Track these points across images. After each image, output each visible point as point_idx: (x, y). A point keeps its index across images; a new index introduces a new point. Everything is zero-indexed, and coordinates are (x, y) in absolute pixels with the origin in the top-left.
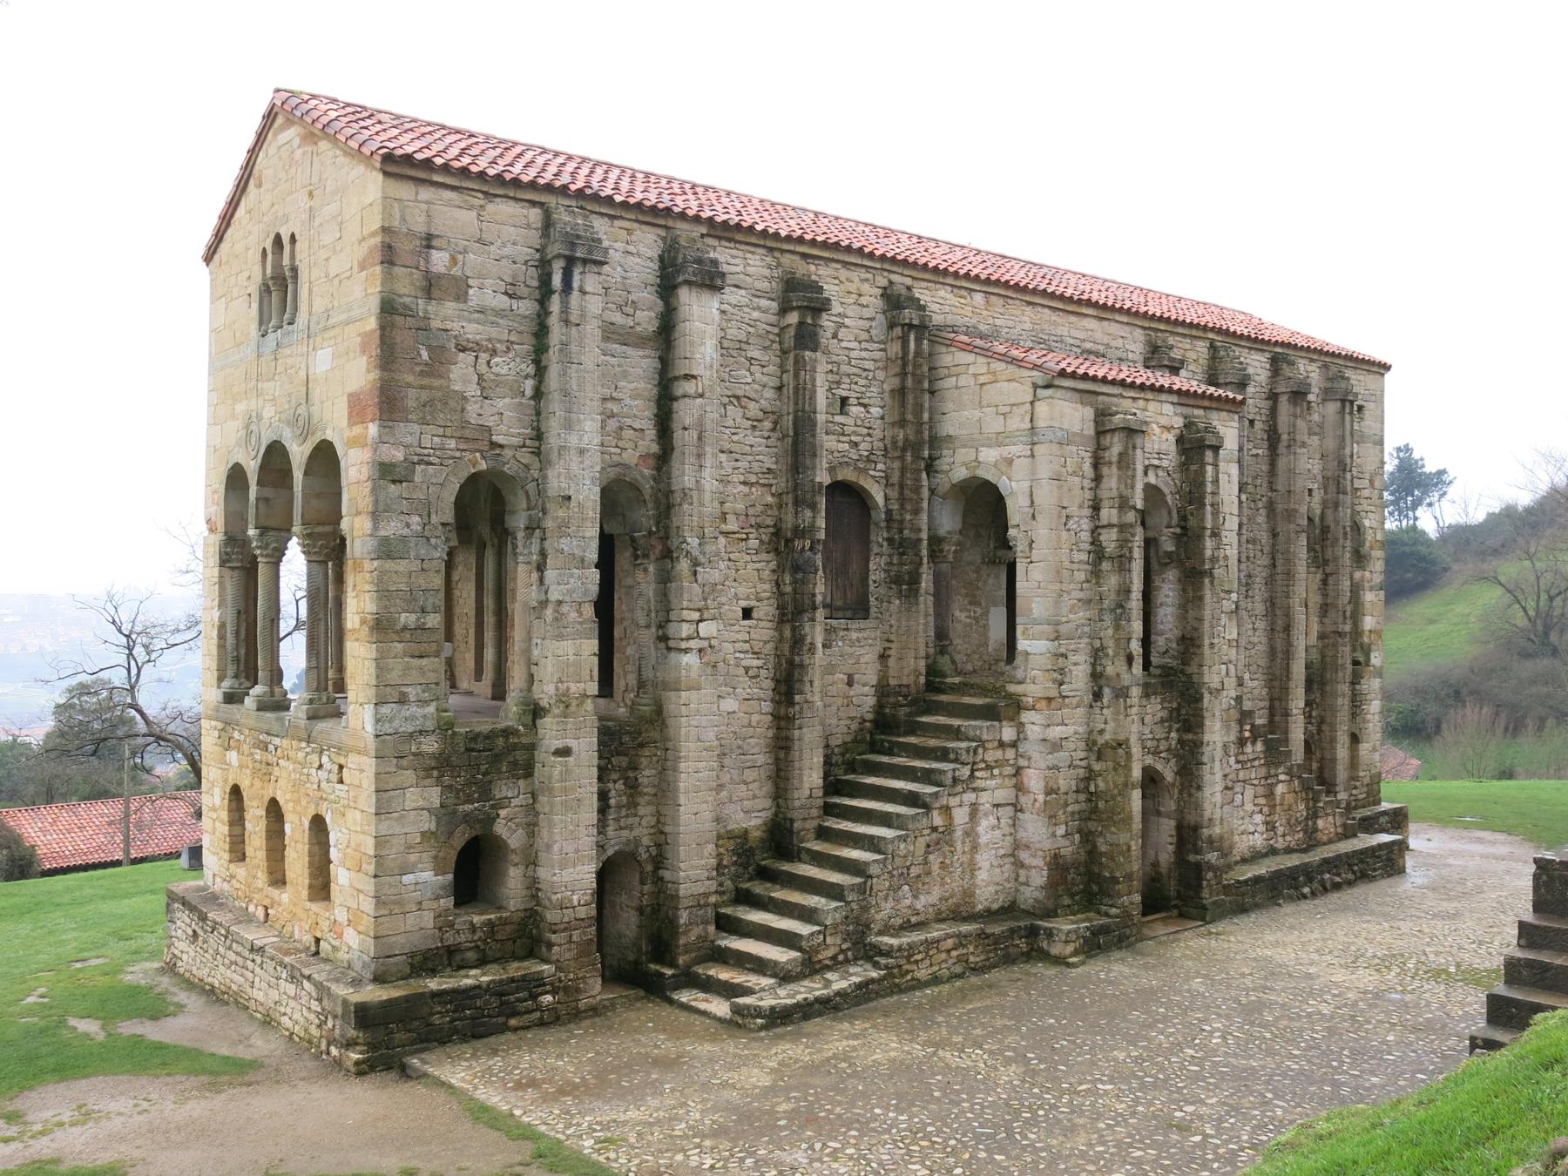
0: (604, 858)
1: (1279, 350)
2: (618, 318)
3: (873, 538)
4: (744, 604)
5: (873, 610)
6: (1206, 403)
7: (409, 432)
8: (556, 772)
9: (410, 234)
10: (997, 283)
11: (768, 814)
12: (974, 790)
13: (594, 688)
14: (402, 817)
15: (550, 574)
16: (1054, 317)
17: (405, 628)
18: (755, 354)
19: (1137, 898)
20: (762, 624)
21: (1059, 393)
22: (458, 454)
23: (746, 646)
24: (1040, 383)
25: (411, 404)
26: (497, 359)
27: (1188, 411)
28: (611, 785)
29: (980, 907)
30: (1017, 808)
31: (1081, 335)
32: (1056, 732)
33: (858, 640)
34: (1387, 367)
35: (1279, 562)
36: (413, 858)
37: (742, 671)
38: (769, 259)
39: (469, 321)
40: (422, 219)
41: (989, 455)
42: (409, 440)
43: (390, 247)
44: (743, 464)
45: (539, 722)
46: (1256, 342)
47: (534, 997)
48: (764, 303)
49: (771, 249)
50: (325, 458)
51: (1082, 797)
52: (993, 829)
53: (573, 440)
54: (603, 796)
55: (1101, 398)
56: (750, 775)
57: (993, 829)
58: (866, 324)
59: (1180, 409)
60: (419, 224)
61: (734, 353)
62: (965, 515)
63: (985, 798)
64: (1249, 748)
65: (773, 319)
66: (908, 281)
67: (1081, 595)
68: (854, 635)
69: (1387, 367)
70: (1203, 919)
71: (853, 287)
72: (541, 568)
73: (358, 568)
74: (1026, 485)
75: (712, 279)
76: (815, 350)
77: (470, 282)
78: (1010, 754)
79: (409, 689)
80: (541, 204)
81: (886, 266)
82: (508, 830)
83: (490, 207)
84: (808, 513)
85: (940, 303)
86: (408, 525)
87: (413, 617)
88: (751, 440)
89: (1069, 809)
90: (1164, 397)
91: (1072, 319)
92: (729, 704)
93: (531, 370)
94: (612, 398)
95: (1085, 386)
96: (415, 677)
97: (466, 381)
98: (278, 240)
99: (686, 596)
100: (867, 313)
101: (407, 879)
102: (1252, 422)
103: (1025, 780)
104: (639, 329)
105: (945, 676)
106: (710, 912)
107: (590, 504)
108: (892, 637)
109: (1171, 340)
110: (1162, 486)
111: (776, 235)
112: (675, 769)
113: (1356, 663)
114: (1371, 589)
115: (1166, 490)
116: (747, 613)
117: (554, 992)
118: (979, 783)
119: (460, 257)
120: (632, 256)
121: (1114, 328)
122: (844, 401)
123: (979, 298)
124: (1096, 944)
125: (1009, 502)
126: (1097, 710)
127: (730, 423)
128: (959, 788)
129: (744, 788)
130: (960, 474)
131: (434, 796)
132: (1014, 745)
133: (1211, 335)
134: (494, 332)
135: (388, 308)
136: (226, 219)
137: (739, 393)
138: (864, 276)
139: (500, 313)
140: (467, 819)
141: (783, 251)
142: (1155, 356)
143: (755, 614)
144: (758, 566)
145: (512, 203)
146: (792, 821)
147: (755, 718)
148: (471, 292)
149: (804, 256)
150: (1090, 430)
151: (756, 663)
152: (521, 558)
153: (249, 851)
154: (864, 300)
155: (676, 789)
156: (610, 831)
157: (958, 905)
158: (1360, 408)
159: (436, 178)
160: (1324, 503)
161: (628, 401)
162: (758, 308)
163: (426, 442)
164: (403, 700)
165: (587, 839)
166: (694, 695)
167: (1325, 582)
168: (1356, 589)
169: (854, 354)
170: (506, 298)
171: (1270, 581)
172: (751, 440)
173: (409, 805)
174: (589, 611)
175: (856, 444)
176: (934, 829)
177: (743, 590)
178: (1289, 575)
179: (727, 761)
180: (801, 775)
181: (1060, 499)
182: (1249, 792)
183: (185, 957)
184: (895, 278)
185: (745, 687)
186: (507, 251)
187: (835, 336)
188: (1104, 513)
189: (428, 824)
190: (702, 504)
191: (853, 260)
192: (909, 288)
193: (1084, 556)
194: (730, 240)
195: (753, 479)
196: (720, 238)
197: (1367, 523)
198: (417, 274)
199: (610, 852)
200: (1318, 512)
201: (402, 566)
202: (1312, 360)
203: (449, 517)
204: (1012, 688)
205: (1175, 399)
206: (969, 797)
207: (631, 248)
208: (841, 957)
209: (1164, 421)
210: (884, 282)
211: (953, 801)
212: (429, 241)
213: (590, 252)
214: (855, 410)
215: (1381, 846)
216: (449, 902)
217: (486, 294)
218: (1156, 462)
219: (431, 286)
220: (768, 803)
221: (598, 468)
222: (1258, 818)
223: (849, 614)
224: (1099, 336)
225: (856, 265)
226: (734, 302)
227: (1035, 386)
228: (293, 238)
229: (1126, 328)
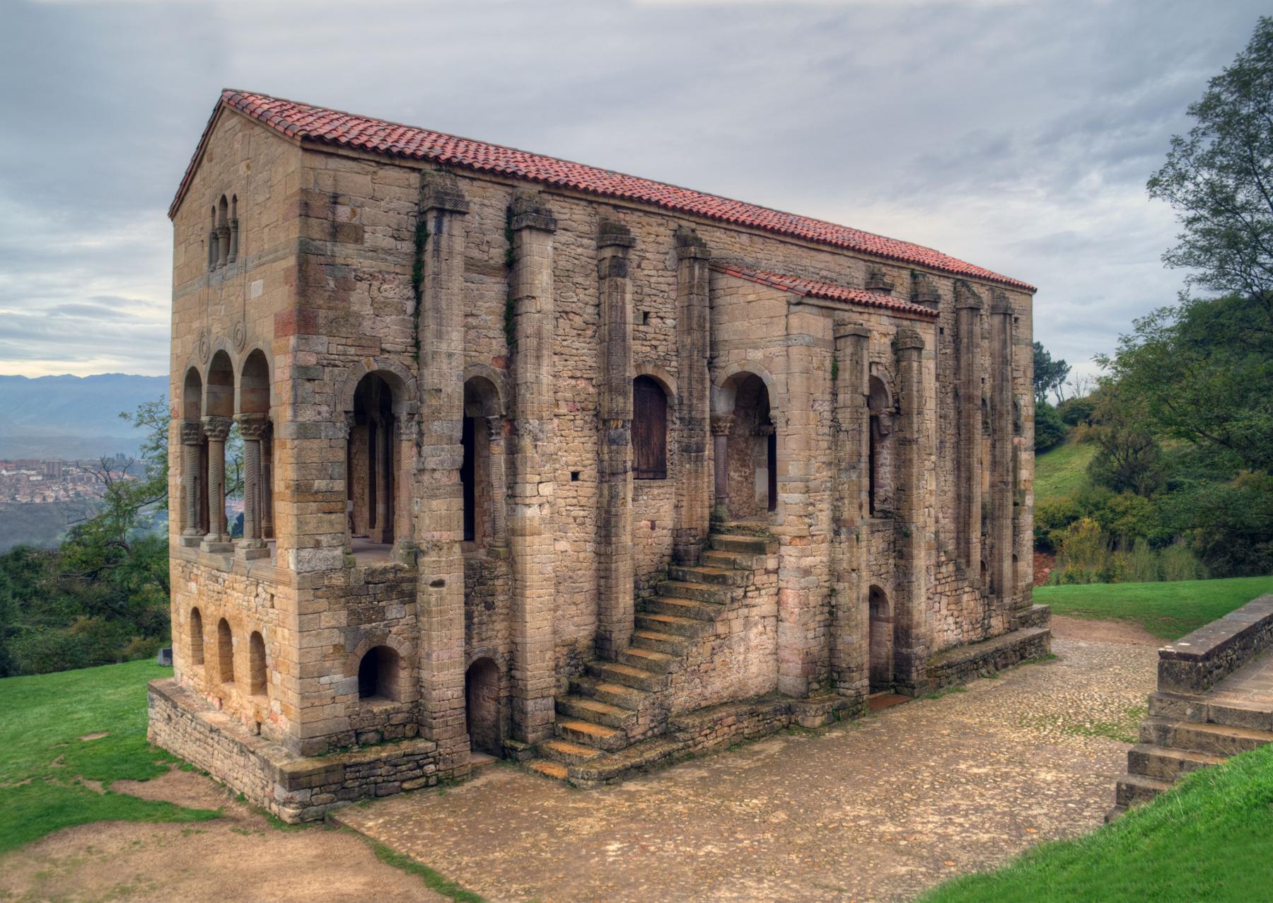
0: (471, 662)
1: (959, 277)
2: (476, 253)
3: (669, 417)
4: (572, 469)
5: (669, 472)
6: (913, 316)
7: (321, 343)
8: (433, 599)
9: (322, 193)
10: (758, 227)
11: (591, 628)
12: (746, 606)
13: (460, 534)
14: (319, 634)
15: (426, 449)
16: (800, 252)
17: (316, 492)
18: (580, 280)
19: (866, 682)
20: (586, 484)
21: (808, 309)
22: (356, 358)
23: (574, 501)
24: (793, 301)
25: (321, 321)
26: (385, 286)
27: (900, 322)
28: (474, 608)
29: (752, 693)
30: (779, 619)
32: (808, 561)
33: (659, 495)
34: (1034, 290)
35: (963, 432)
36: (328, 664)
37: (571, 520)
38: (589, 209)
39: (366, 258)
40: (330, 182)
41: (757, 355)
42: (320, 348)
43: (306, 204)
44: (571, 363)
45: (419, 560)
46: (943, 271)
47: (421, 767)
48: (585, 241)
49: (591, 202)
50: (258, 364)
51: (826, 609)
52: (761, 634)
53: (444, 347)
54: (469, 616)
56: (579, 598)
57: (761, 634)
58: (662, 257)
59: (893, 321)
60: (328, 185)
61: (564, 279)
62: (737, 400)
63: (755, 611)
64: (944, 569)
65: (592, 253)
66: (693, 226)
67: (824, 459)
68: (656, 491)
69: (1034, 290)
70: (912, 695)
71: (654, 229)
72: (419, 445)
73: (283, 446)
74: (783, 377)
75: (547, 224)
76: (624, 277)
77: (366, 228)
78: (773, 578)
79: (322, 538)
80: (419, 170)
81: (677, 215)
82: (397, 642)
83: (382, 173)
84: (621, 400)
85: (718, 242)
86: (319, 413)
87: (324, 482)
88: (577, 345)
89: (818, 618)
90: (882, 311)
91: (813, 253)
92: (562, 545)
93: (411, 293)
94: (472, 315)
95: (824, 302)
96: (325, 528)
97: (363, 304)
98: (224, 201)
99: (529, 464)
100: (663, 249)
101: (324, 680)
102: (942, 329)
103: (784, 598)
104: (492, 262)
105: (722, 521)
106: (551, 701)
107: (456, 395)
108: (684, 493)
109: (884, 269)
111: (595, 192)
112: (523, 595)
113: (1015, 504)
114: (1026, 450)
115: (885, 381)
116: (575, 476)
117: (435, 763)
118: (748, 601)
119: (358, 210)
120: (487, 206)
121: (842, 260)
122: (646, 315)
123: (744, 239)
125: (770, 389)
126: (837, 545)
127: (561, 332)
128: (736, 605)
129: (574, 607)
130: (734, 369)
131: (342, 617)
132: (776, 571)
133: (912, 266)
134: (383, 266)
135: (306, 252)
136: (186, 185)
137: (568, 309)
139: (388, 252)
140: (369, 634)
141: (600, 204)
142: (875, 283)
143: (581, 477)
144: (583, 440)
145: (397, 169)
146: (611, 632)
147: (582, 555)
148: (366, 236)
149: (615, 207)
150: (829, 336)
151: (582, 513)
152: (404, 437)
153: (207, 656)
154: (660, 239)
155: (524, 611)
156: (475, 642)
157: (735, 692)
158: (1016, 319)
159: (341, 152)
160: (993, 388)
161: (484, 317)
162: (581, 246)
163: (333, 349)
164: (317, 545)
165: (458, 648)
166: (536, 539)
167: (994, 446)
168: (1016, 450)
169: (653, 280)
170: (392, 240)
171: (957, 446)
172: (577, 345)
173: (323, 624)
174: (456, 477)
175: (656, 347)
176: (718, 636)
177: (572, 458)
178: (970, 440)
179: (561, 588)
180: (617, 598)
181: (808, 388)
182: (944, 601)
183: (163, 734)
184: (683, 223)
185: (574, 532)
186: (392, 206)
187: (639, 266)
188: (841, 397)
189: (338, 639)
190: (540, 394)
192: (693, 231)
193: (826, 430)
195: (578, 374)
196: (553, 194)
197: (1022, 403)
198: (326, 224)
199: (475, 658)
200: (989, 395)
201: (315, 444)
202: (983, 285)
203: (350, 407)
204: (774, 530)
205: (890, 313)
206: (744, 611)
207: (486, 202)
208: (650, 733)
209: (882, 329)
210: (673, 225)
211: (732, 615)
212: (335, 200)
213: (456, 205)
214: (654, 321)
215: (1034, 638)
216: (353, 697)
217: (378, 237)
218: (877, 360)
219: (336, 231)
220: (592, 619)
221: (462, 368)
222: (951, 620)
223: (651, 475)
224: (832, 266)
226: (563, 239)
227: (789, 303)
228: (235, 199)
229: (852, 261)
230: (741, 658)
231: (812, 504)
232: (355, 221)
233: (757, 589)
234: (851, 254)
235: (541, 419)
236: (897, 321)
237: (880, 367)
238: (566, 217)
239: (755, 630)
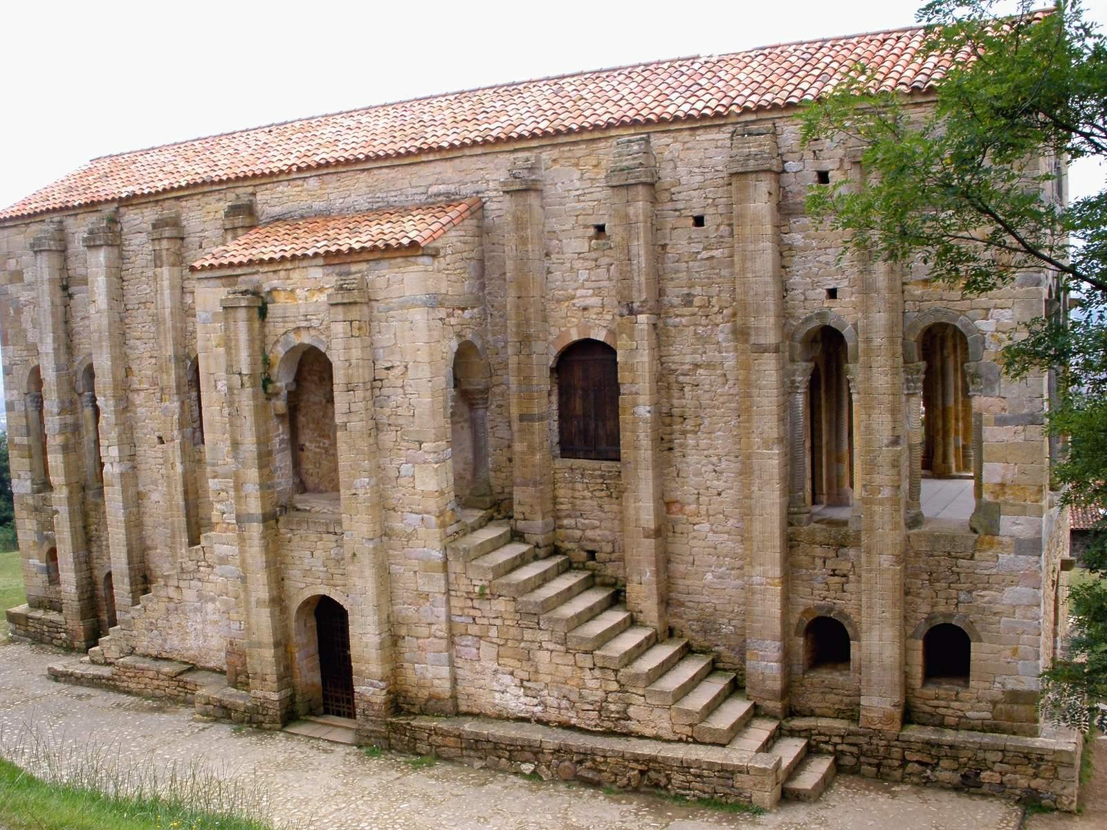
16: (393, 173)
31: (431, 179)
38: (158, 208)
49: (157, 201)
55: (240, 279)
59: (330, 269)
90: (305, 263)
91: (415, 169)
102: (699, 221)
110: (315, 344)
121: (465, 163)
123: (313, 183)
124: (222, 713)
137: (143, 300)
138: (217, 197)
149: (178, 198)
176: (170, 599)
182: (487, 650)
191: (206, 189)
194: (132, 205)
196: (127, 206)
205: (320, 261)
218: (304, 324)
225: (211, 192)
229: (483, 158)
230: (199, 627)
231: (223, 490)
232: (19, 268)
233: (209, 566)
234: (479, 151)
235: (105, 396)
236: (337, 269)
237: (313, 332)
238: (138, 222)
239: (210, 606)
